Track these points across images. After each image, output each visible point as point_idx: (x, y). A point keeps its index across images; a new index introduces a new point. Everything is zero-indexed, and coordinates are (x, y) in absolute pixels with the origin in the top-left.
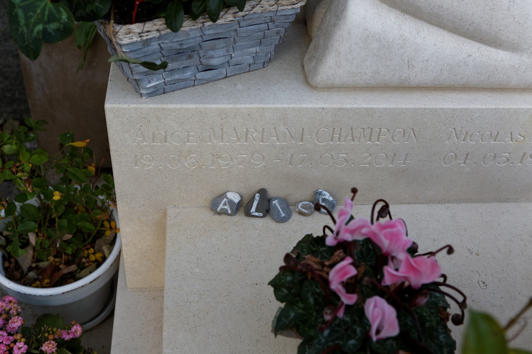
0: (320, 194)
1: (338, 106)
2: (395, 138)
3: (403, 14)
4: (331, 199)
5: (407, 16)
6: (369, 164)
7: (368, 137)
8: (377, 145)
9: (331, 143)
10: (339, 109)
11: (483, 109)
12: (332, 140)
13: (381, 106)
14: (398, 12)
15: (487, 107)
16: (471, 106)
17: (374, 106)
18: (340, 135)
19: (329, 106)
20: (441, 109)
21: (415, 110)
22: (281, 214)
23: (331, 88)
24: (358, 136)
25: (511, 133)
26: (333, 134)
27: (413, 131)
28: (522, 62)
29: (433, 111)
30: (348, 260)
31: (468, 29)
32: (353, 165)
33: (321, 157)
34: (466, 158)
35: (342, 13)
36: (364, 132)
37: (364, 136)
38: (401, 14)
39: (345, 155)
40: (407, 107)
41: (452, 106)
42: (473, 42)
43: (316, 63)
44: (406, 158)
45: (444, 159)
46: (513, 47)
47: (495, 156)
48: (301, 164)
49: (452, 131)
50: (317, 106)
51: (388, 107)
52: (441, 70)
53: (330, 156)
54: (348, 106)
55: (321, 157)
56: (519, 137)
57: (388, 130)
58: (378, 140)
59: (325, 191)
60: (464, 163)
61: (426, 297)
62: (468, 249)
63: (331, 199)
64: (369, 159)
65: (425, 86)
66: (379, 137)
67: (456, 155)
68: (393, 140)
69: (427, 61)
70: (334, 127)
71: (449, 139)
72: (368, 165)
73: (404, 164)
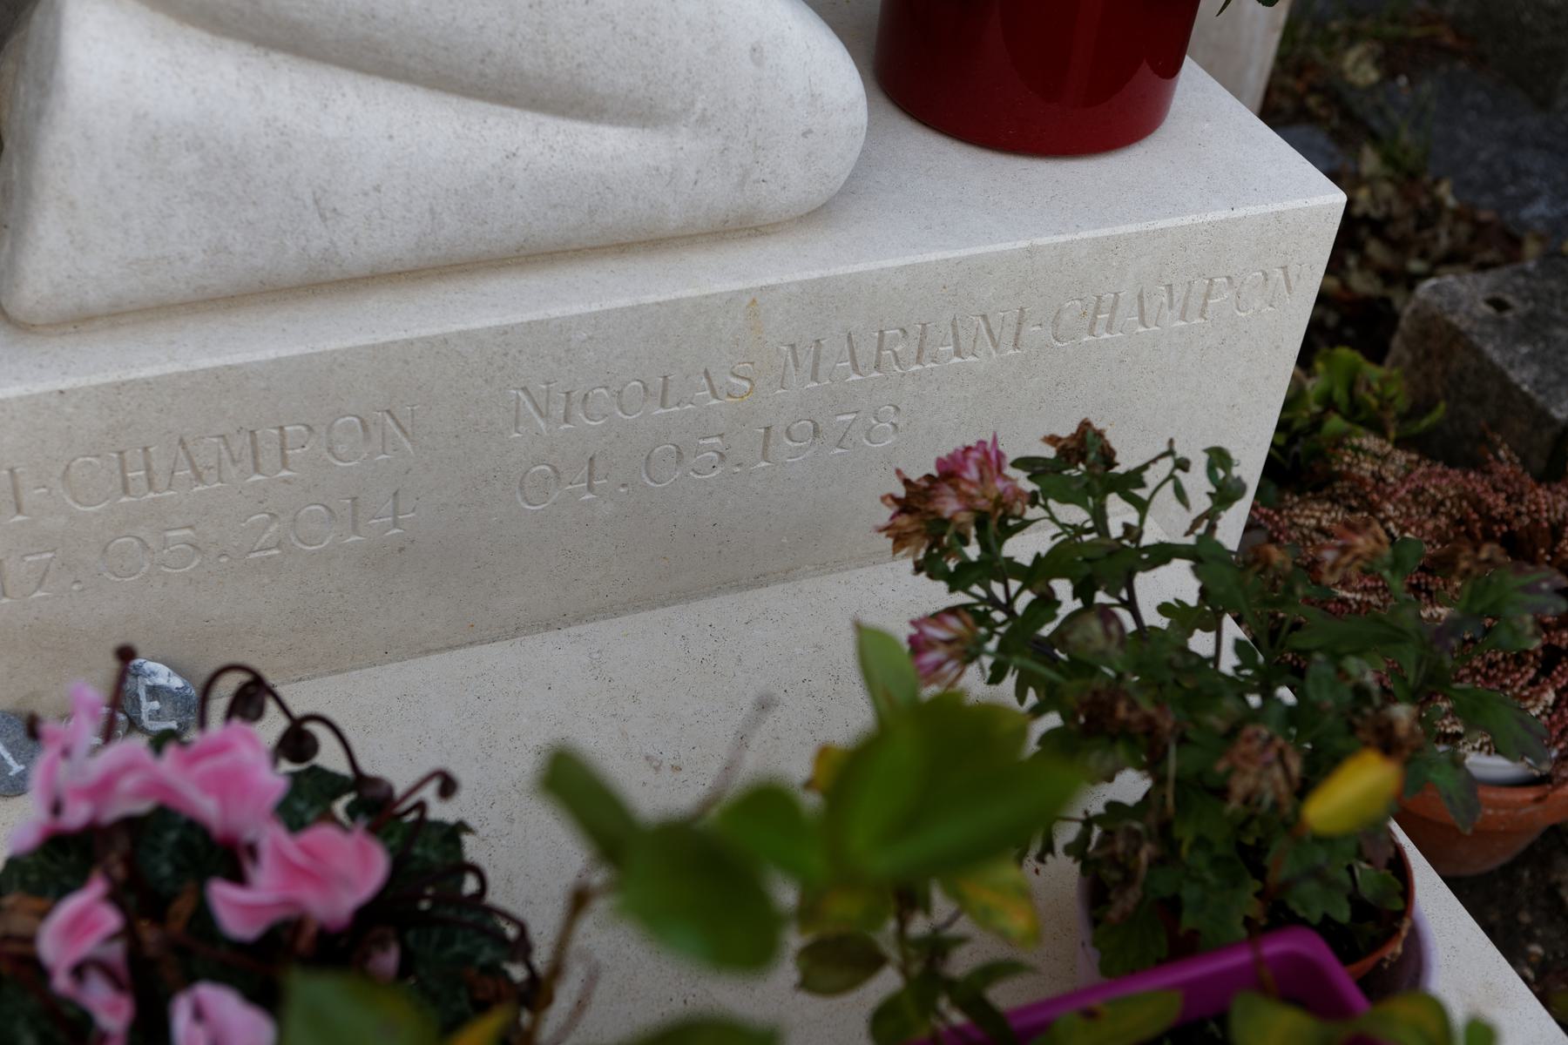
0: (136, 676)
1: (113, 377)
2: (341, 449)
3: (262, 51)
4: (177, 682)
5: (277, 57)
6: (278, 546)
7: (248, 463)
8: (286, 481)
9: (125, 499)
10: (119, 387)
11: (595, 316)
12: (126, 491)
13: (259, 356)
14: (244, 48)
15: (606, 307)
16: (555, 311)
17: (237, 359)
18: (148, 469)
19: (83, 382)
20: (460, 334)
21: (377, 352)
22: (10, 768)
23: (80, 321)
24: (212, 462)
25: (706, 373)
26: (123, 471)
27: (393, 417)
28: (681, 154)
29: (440, 346)
30: (96, 888)
31: (482, 75)
32: (224, 560)
33: (105, 551)
34: (590, 474)
35: (51, 73)
36: (228, 448)
37: (234, 462)
38: (254, 51)
39: (187, 532)
40: (348, 344)
41: (494, 321)
42: (516, 112)
43: (13, 245)
44: (396, 506)
45: (521, 488)
46: (638, 112)
47: (679, 453)
48: (40, 585)
49: (518, 397)
50: (38, 388)
51: (284, 353)
52: (432, 211)
53: (136, 543)
54: (147, 372)
55: (105, 551)
56: (734, 380)
57: (310, 429)
58: (285, 465)
59: (153, 660)
60: (590, 488)
61: (385, 948)
62: (647, 758)
63: (177, 682)
64: (272, 529)
65: (397, 268)
66: (284, 457)
67: (555, 470)
68: (334, 455)
69: (377, 189)
70: (120, 447)
71: (517, 424)
72: (275, 552)
73: (395, 524)
